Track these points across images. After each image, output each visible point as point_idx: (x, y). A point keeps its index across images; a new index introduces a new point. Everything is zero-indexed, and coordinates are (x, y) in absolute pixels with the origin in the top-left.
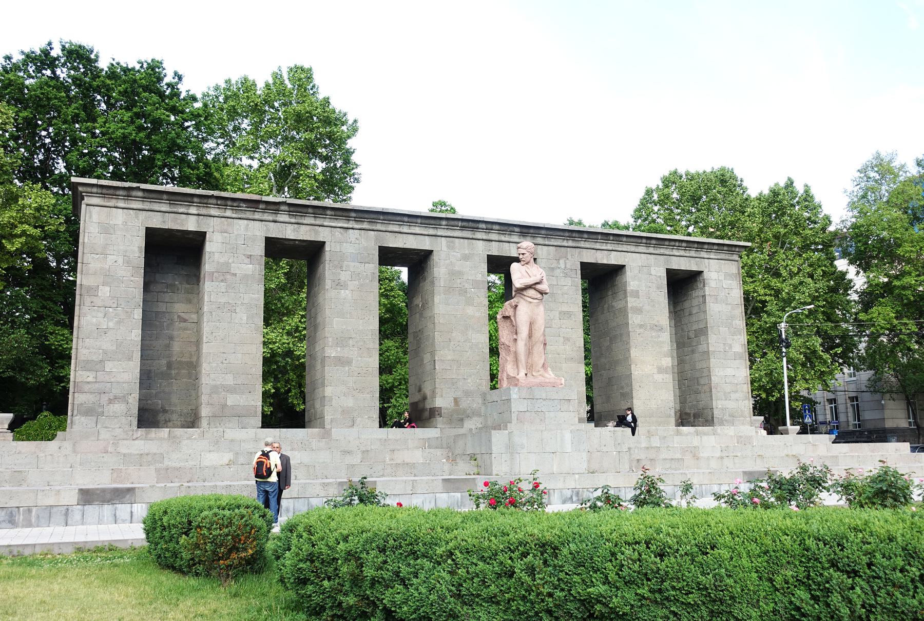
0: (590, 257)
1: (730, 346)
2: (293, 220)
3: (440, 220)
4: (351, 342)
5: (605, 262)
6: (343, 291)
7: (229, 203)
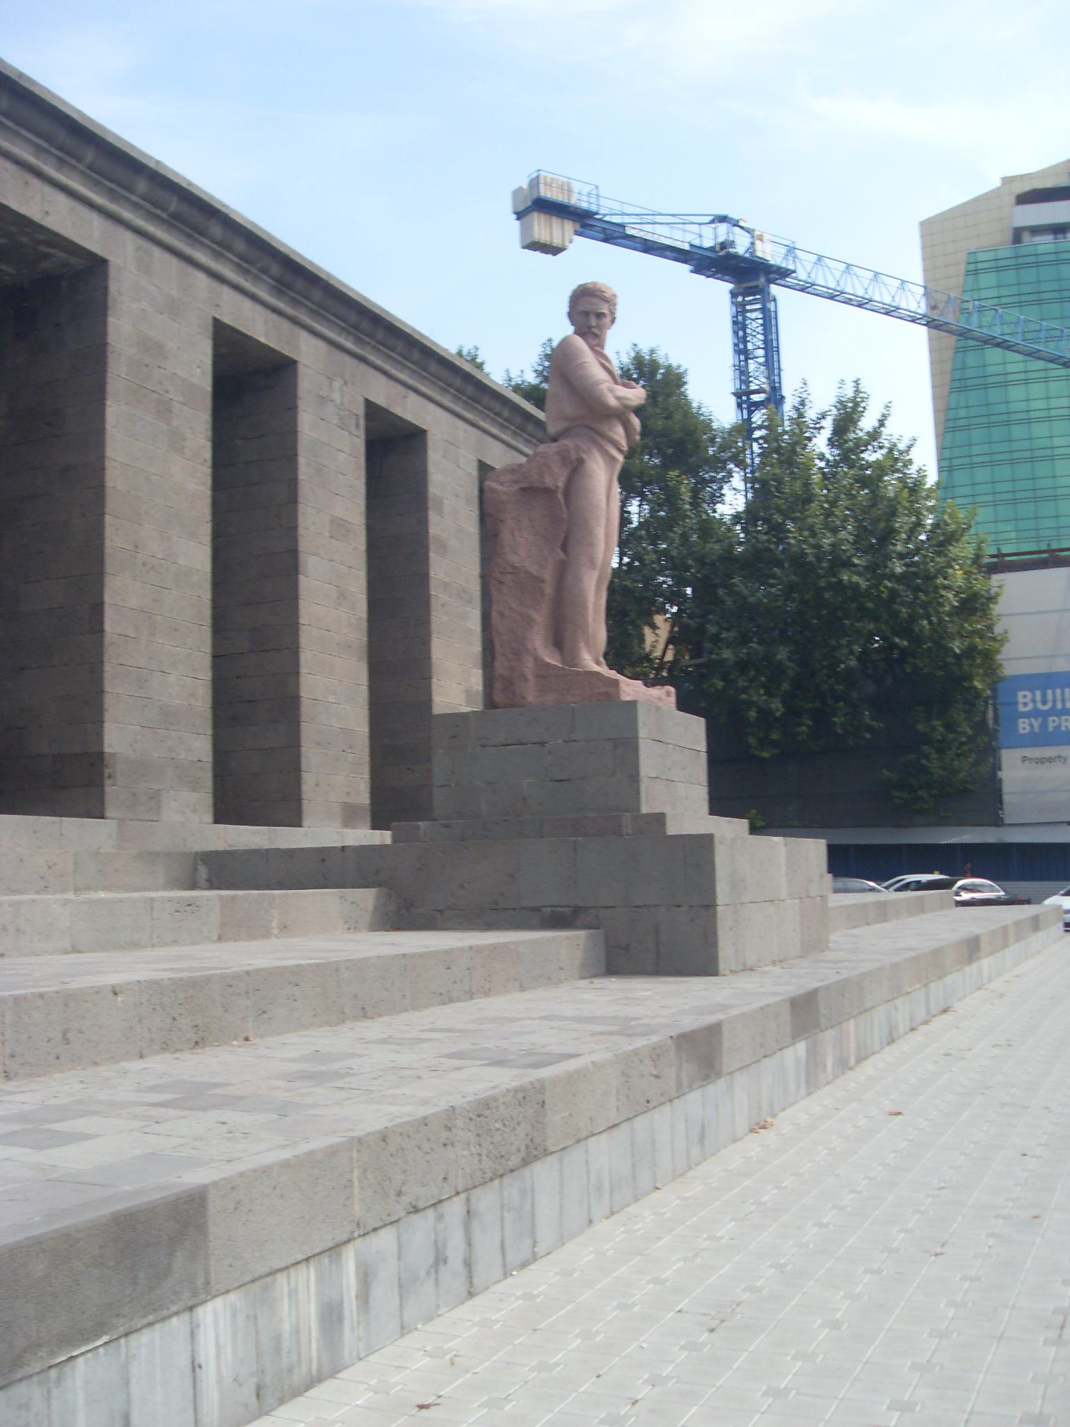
0: (383, 393)
5: (398, 410)
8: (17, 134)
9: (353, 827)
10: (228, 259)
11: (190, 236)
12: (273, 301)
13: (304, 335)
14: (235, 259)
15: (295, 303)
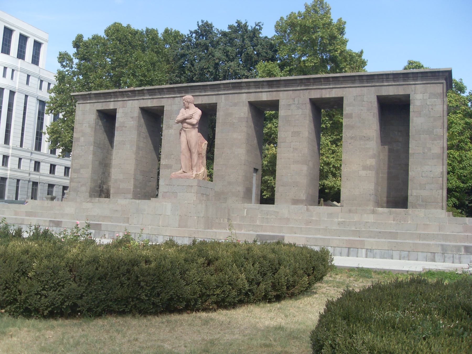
0: (316, 94)
1: (430, 149)
2: (150, 97)
3: (415, 74)
4: (172, 156)
5: (328, 96)
6: (170, 130)
7: (124, 93)
13: (281, 93)
15: (278, 87)
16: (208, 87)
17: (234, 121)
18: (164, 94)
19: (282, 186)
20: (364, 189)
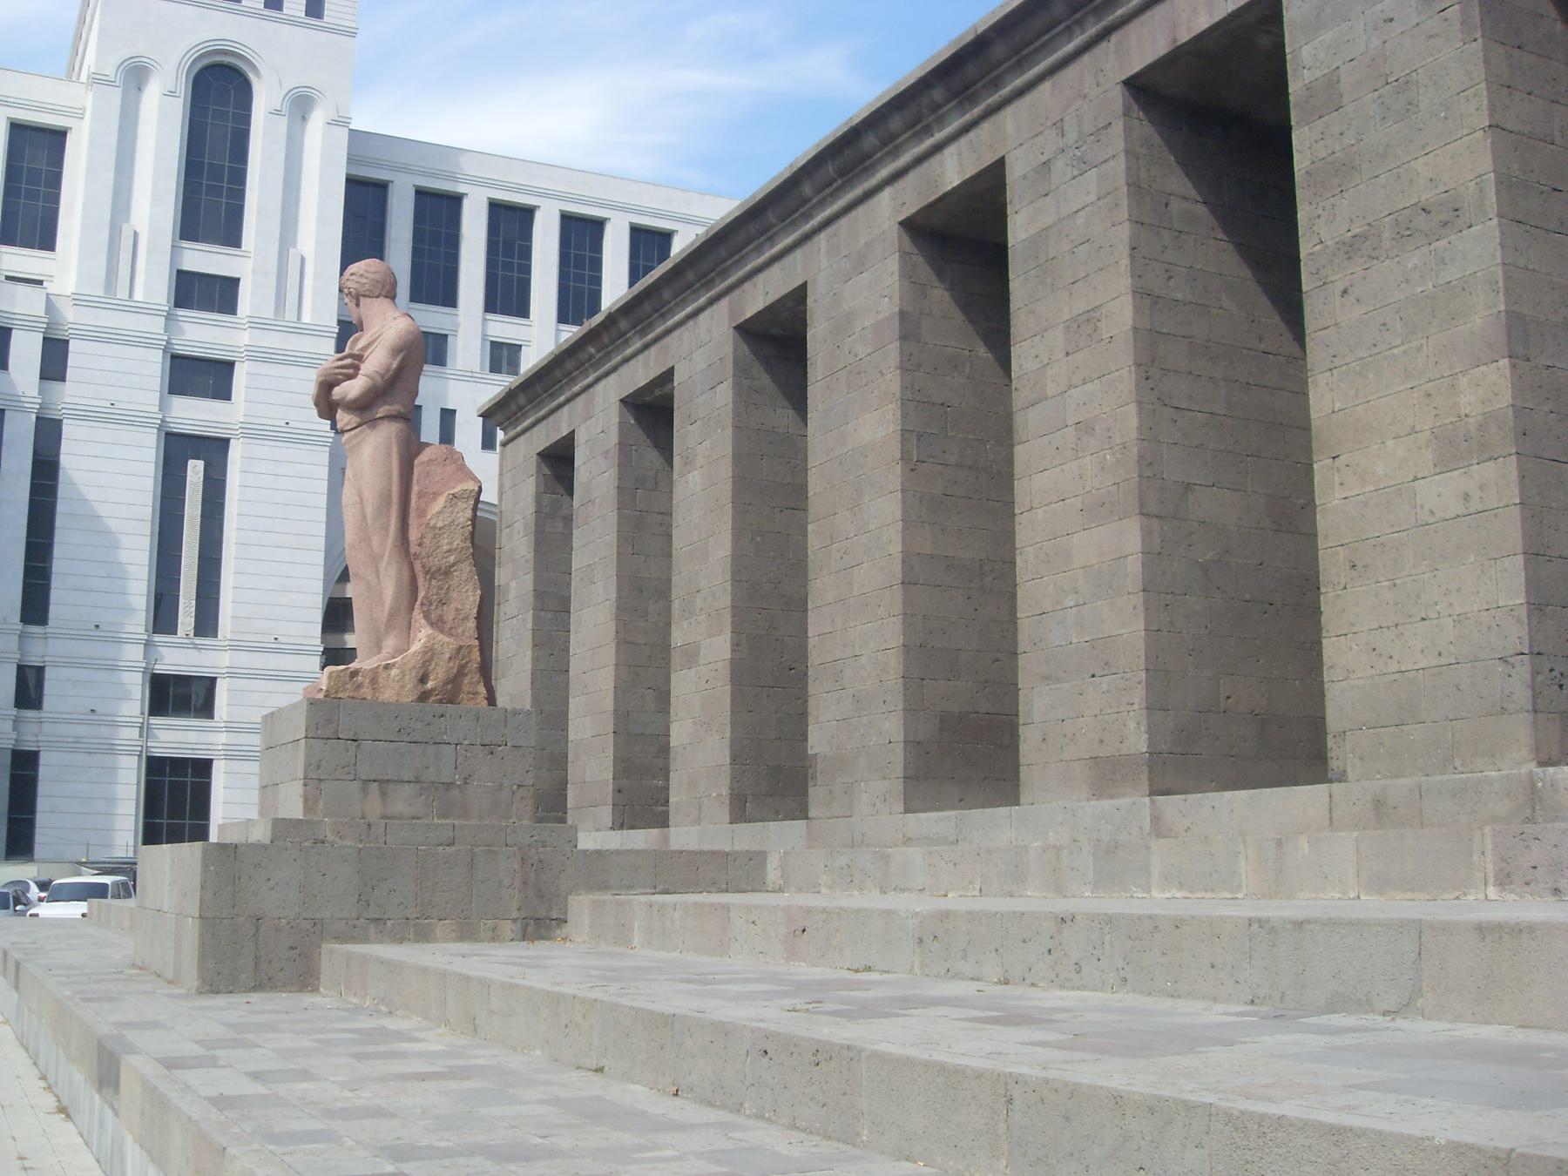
8: (743, 257)
9: (1112, 797)
10: (902, 143)
11: (866, 169)
12: (977, 111)
14: (909, 134)
16: (771, 217)
17: (862, 350)
18: (672, 312)
19: (1046, 678)
20: (1459, 620)
